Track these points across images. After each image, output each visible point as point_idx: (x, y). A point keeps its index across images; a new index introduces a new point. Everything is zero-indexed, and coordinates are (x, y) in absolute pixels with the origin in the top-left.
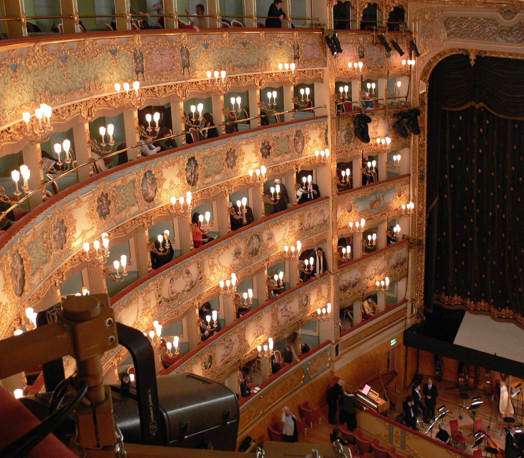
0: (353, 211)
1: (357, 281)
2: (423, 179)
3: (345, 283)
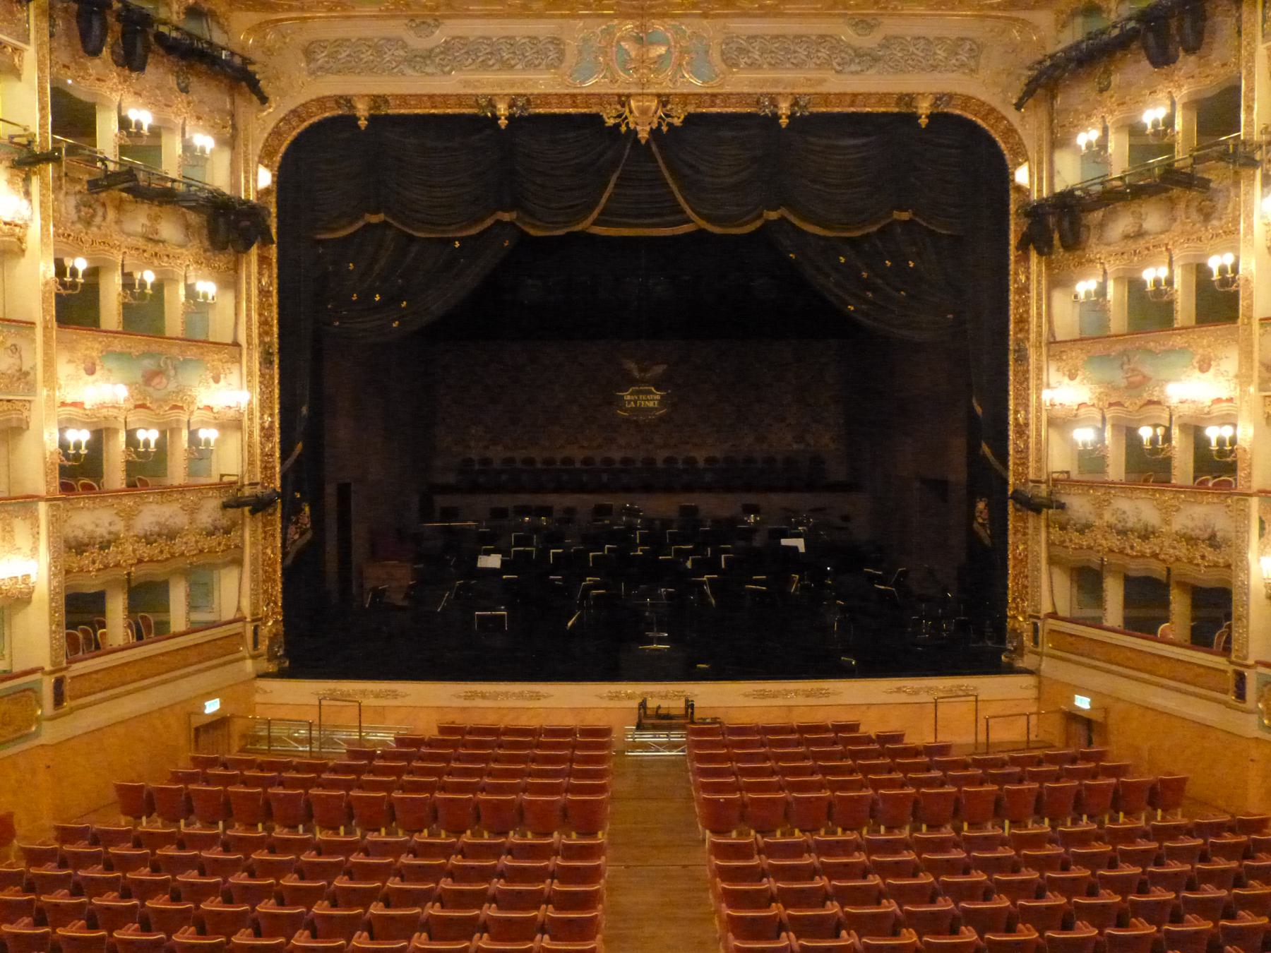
2: (271, 363)
3: (80, 534)
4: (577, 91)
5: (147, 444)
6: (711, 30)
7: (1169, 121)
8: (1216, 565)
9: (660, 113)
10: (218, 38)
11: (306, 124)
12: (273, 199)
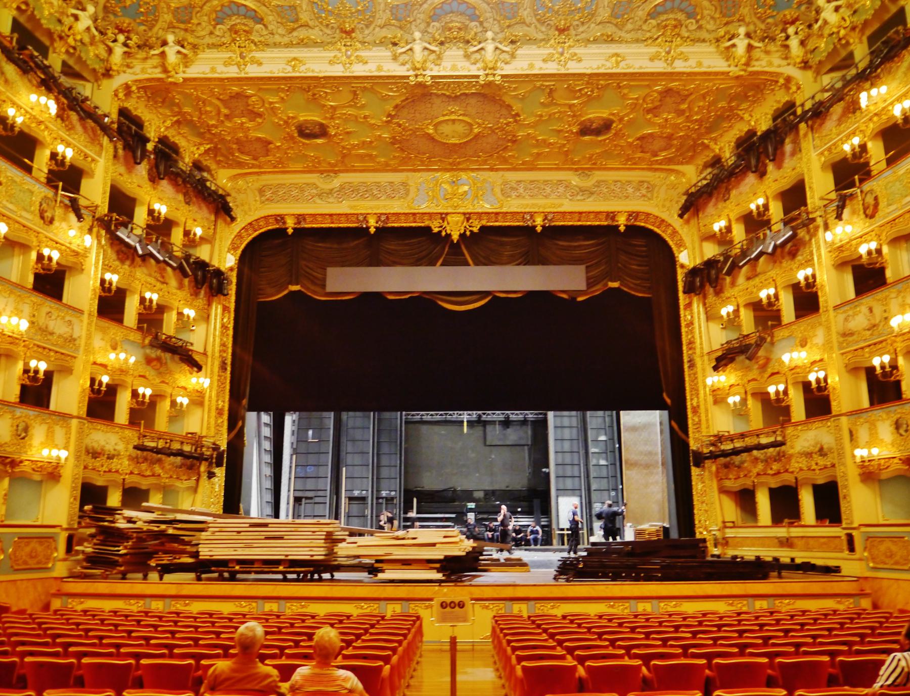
1: (115, 453)
2: (226, 369)
3: (96, 445)
5: (144, 395)
6: (495, 178)
12: (234, 274)
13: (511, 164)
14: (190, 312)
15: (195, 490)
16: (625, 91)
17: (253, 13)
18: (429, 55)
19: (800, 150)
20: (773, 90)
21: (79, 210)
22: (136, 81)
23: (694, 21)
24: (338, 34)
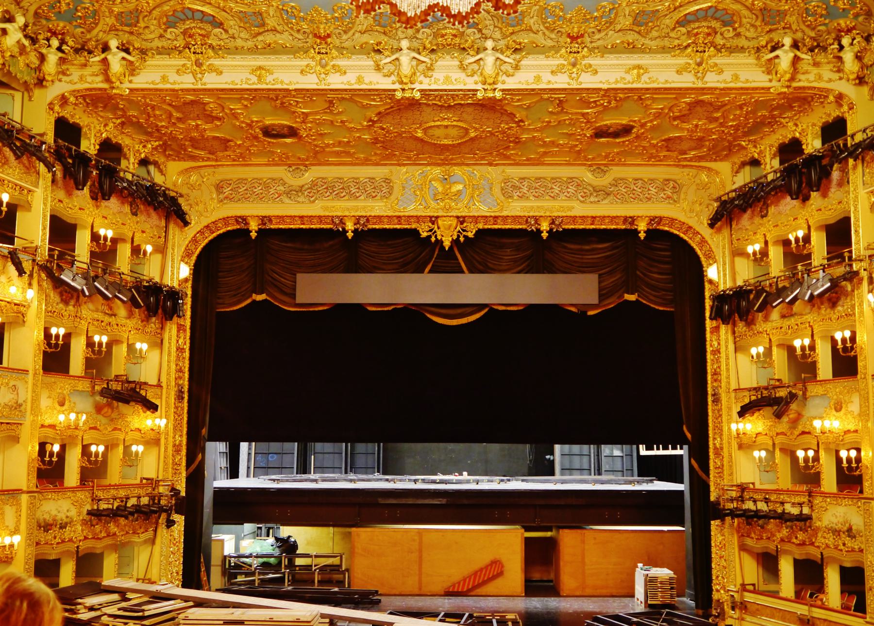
0: (67, 403)
2: (183, 398)
4: (402, 214)
6: (494, 174)
7: (807, 239)
8: (853, 550)
9: (458, 228)
10: (158, 179)
11: (215, 235)
12: (189, 284)
13: (514, 160)
14: (142, 346)
15: (153, 541)
16: (649, 102)
17: (211, 18)
18: (417, 65)
19: (848, 182)
20: (822, 103)
21: (20, 263)
22: (74, 91)
23: (731, 29)
24: (311, 40)
